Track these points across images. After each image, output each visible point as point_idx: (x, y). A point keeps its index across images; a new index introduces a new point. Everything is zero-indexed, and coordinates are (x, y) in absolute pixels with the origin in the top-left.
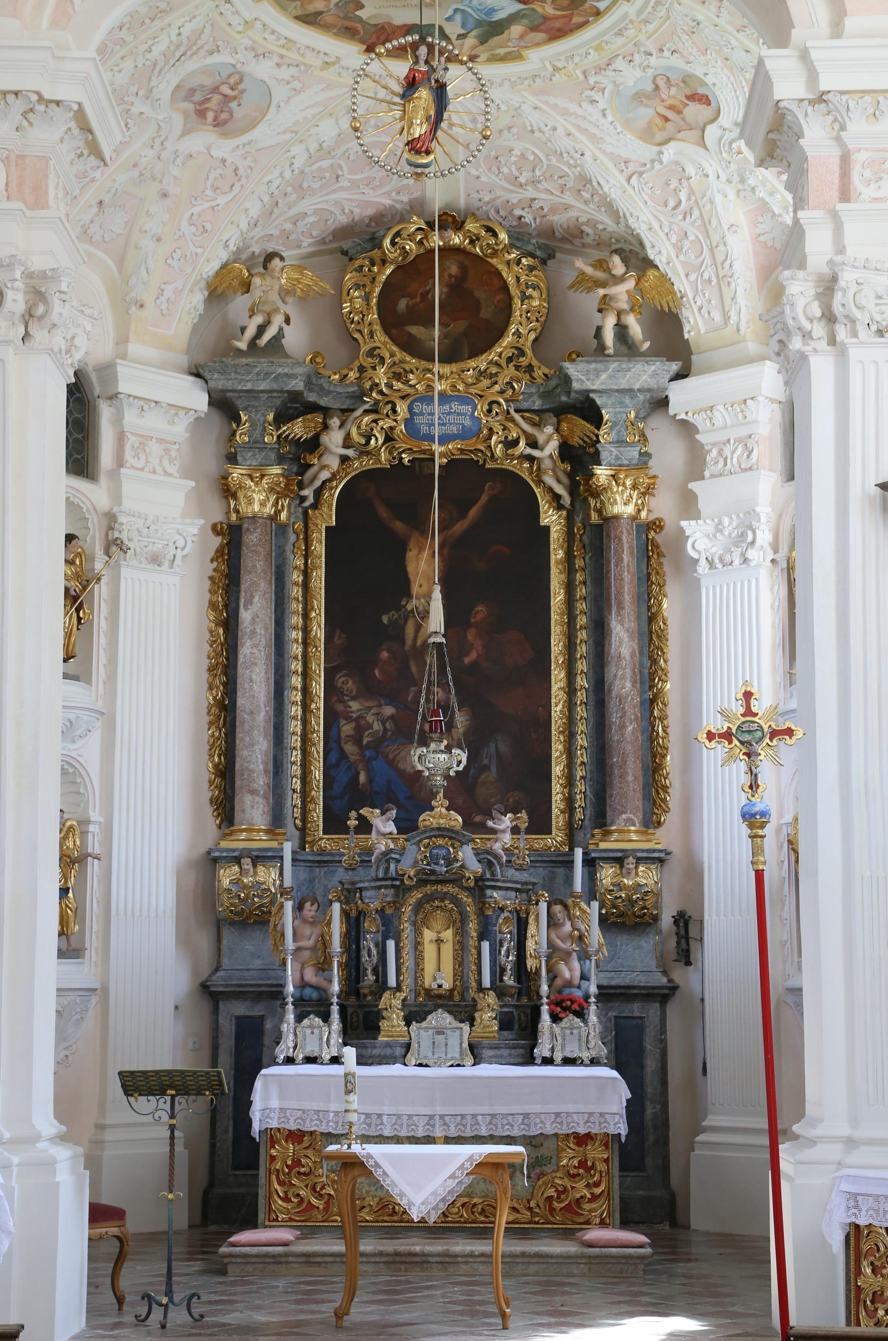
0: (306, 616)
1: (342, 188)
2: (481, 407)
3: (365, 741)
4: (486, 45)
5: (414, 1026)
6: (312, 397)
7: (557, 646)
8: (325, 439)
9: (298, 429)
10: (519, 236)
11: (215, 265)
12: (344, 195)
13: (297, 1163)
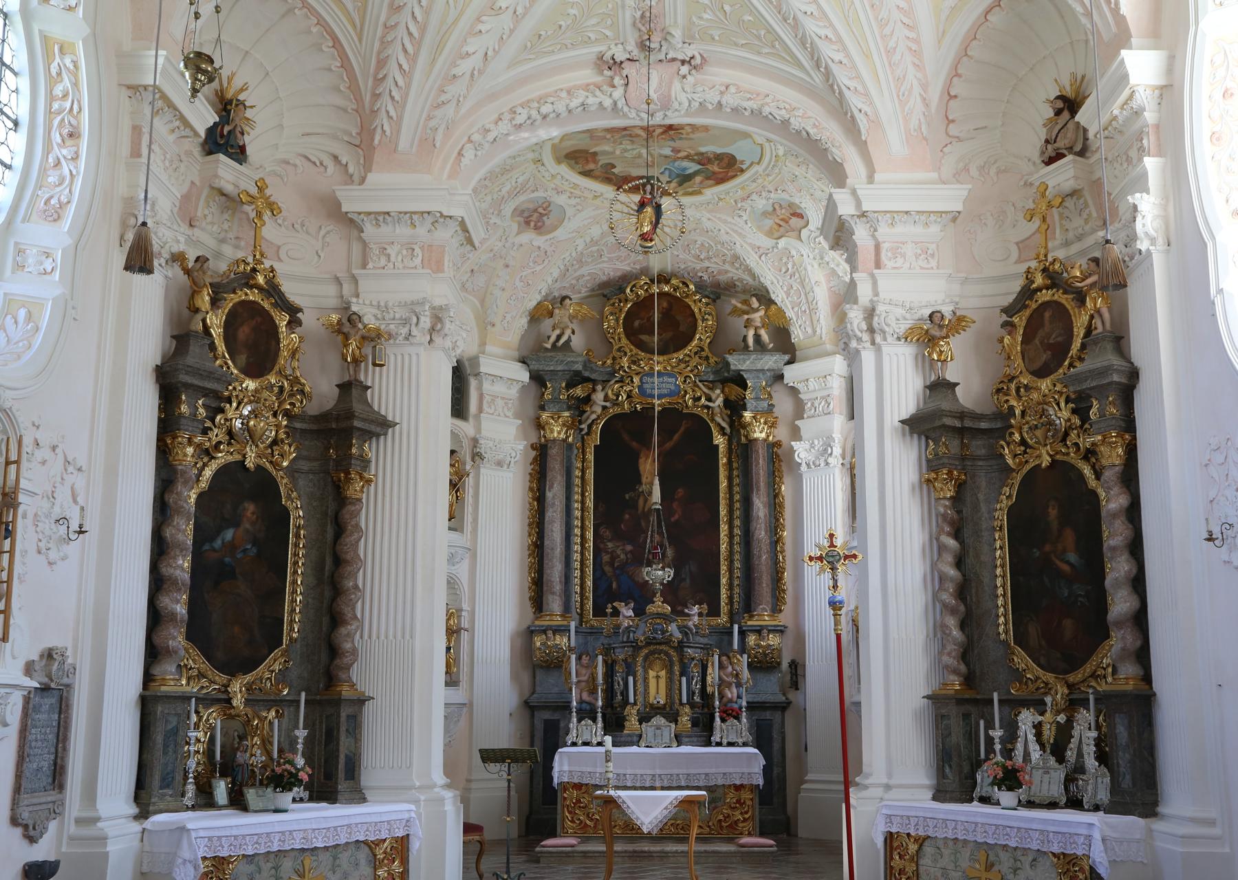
0: (583, 495)
1: (604, 262)
2: (680, 379)
3: (616, 565)
5: (644, 725)
6: (586, 374)
7: (723, 512)
8: (594, 397)
9: (579, 391)
10: (700, 287)
11: (534, 303)
12: (605, 265)
13: (579, 801)
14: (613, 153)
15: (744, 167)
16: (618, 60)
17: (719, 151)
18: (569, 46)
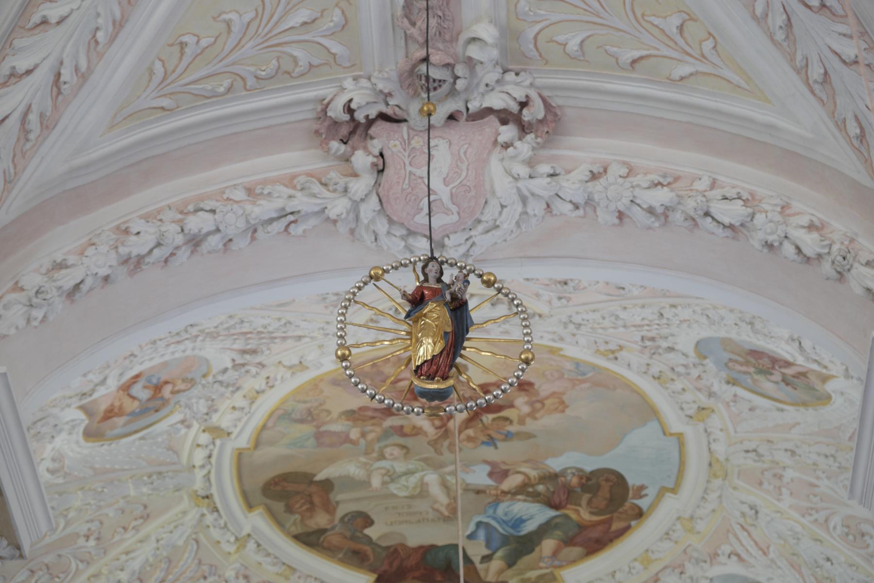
4: (515, 567)
14: (365, 484)
15: (643, 503)
16: (360, 116)
17: (589, 466)
18: (251, 82)
